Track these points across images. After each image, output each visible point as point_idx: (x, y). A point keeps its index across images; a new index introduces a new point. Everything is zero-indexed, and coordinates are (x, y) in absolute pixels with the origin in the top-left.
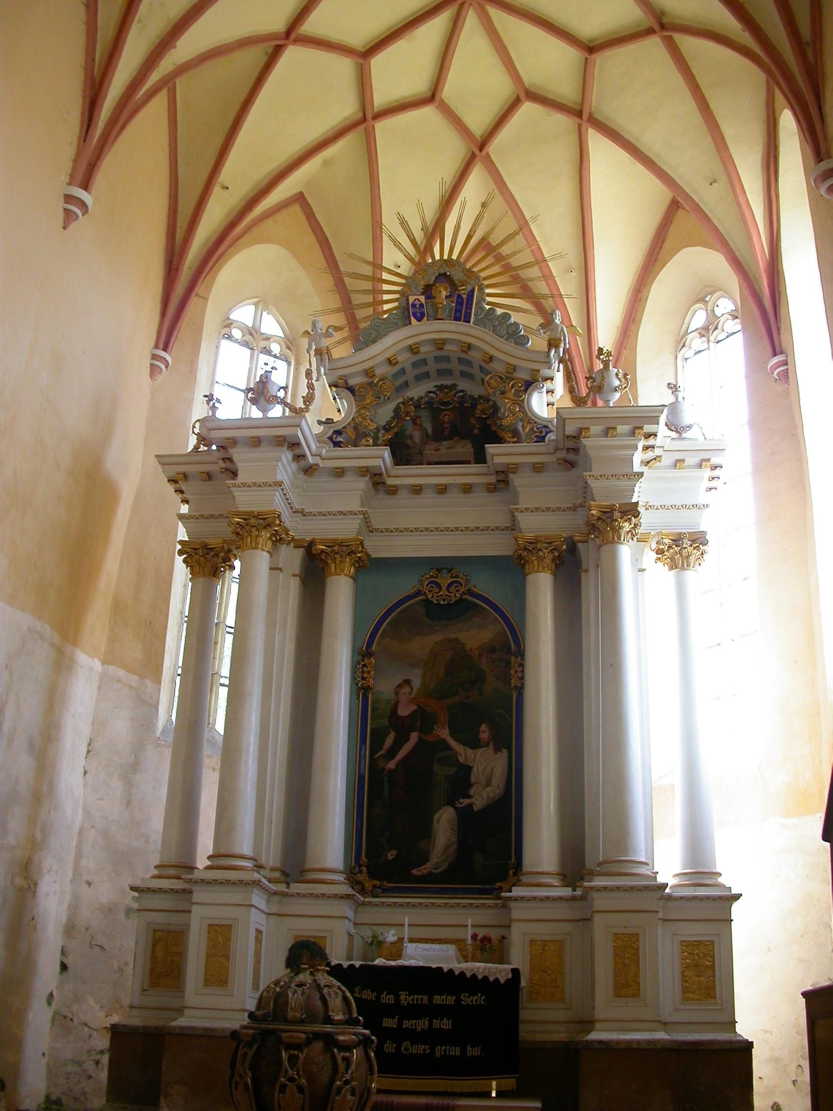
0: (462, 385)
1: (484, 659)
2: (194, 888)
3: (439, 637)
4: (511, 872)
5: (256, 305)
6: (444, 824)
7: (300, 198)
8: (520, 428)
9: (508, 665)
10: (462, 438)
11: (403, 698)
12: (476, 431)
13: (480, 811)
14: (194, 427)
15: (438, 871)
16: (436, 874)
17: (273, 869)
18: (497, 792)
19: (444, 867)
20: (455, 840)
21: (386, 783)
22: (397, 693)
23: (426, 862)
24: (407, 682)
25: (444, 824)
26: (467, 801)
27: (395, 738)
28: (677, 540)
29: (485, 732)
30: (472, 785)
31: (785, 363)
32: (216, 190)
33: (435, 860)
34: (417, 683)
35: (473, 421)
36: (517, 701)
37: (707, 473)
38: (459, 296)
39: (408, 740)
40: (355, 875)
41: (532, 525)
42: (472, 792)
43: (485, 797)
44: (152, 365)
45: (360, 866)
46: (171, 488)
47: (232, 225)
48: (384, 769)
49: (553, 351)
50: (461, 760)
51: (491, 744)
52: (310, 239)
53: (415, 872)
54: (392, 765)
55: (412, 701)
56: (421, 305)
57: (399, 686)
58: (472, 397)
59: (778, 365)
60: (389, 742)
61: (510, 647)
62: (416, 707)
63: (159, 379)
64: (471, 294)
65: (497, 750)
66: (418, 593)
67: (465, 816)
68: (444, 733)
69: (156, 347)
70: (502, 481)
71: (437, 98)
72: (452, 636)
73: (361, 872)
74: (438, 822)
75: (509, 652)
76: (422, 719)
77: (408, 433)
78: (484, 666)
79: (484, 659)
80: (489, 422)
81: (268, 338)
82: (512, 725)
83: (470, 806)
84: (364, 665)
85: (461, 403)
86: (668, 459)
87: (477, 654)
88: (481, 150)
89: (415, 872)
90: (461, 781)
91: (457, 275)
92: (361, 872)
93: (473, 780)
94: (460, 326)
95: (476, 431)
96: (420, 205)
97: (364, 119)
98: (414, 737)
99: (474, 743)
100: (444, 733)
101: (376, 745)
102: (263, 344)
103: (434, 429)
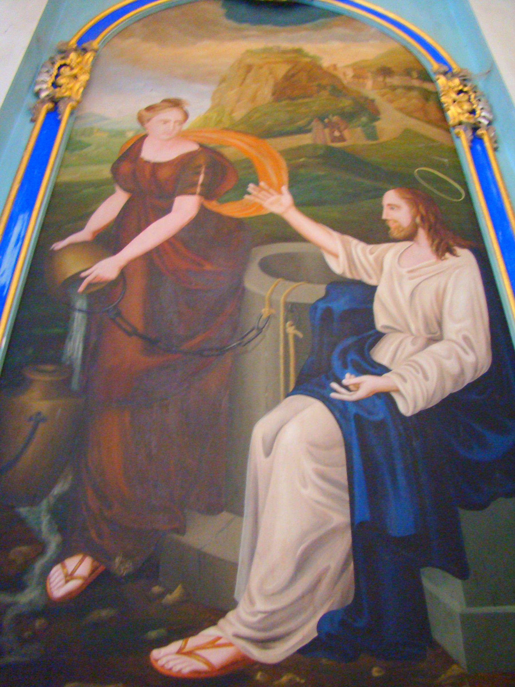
1: (369, 83)
13: (423, 415)
18: (470, 359)
20: (340, 517)
26: (368, 384)
27: (125, 212)
30: (379, 336)
34: (199, 104)
42: (382, 354)
43: (433, 373)
50: (338, 266)
51: (422, 234)
57: (150, 109)
60: (107, 212)
62: (194, 147)
65: (443, 248)
67: (370, 433)
68: (278, 202)
74: (268, 452)
78: (369, 89)
79: (369, 83)
82: (469, 199)
83: (386, 398)
87: (350, 73)
89: (169, 658)
93: (381, 321)
98: (185, 207)
100: (278, 202)
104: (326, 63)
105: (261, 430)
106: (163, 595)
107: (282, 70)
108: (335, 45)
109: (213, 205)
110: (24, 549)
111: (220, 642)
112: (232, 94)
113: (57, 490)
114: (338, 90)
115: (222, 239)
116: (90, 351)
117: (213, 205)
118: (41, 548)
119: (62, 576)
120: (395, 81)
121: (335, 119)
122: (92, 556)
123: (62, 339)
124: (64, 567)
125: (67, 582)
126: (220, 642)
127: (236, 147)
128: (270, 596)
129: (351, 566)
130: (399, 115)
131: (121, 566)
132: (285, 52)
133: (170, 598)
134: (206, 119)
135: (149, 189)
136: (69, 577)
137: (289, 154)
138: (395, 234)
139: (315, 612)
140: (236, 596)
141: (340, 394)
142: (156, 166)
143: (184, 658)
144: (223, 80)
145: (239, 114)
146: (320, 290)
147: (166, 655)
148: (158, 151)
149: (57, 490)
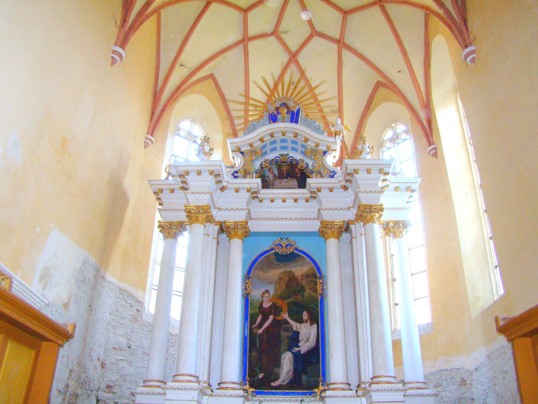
0: (292, 154)
1: (304, 281)
2: (167, 392)
3: (281, 270)
4: (321, 383)
5: (191, 121)
6: (287, 361)
7: (212, 76)
8: (322, 171)
9: (316, 283)
10: (292, 178)
11: (266, 299)
12: (298, 175)
13: (304, 354)
14: (166, 169)
15: (284, 384)
16: (284, 385)
17: (204, 382)
18: (312, 344)
19: (287, 381)
20: (292, 368)
21: (258, 340)
22: (262, 297)
24: (267, 291)
25: (287, 361)
26: (297, 349)
27: (262, 320)
28: (396, 223)
29: (305, 316)
30: (299, 341)
31: (436, 148)
32: (177, 66)
34: (272, 292)
35: (297, 170)
36: (321, 300)
37: (409, 193)
38: (293, 112)
39: (268, 319)
41: (327, 216)
42: (300, 344)
43: (306, 347)
44: (145, 142)
46: (154, 197)
47: (183, 83)
48: (256, 333)
49: (337, 137)
50: (294, 329)
52: (216, 94)
53: (273, 384)
54: (260, 331)
55: (270, 300)
56: (275, 116)
57: (263, 293)
58: (296, 160)
59: (433, 149)
61: (316, 275)
63: (148, 149)
64: (299, 109)
65: (312, 324)
66: (272, 249)
67: (297, 357)
68: (286, 316)
69: (148, 134)
70: (314, 196)
71: (276, 32)
72: (288, 270)
75: (316, 277)
76: (275, 309)
77: (266, 175)
78: (304, 283)
79: (304, 281)
80: (304, 171)
81: (196, 137)
83: (299, 351)
84: (246, 283)
85: (291, 162)
86: (392, 186)
88: (294, 57)
90: (295, 339)
91: (291, 104)
93: (300, 338)
94: (294, 125)
95: (298, 175)
96: (272, 74)
97: (243, 40)
98: (271, 318)
99: (300, 321)
100: (286, 316)
101: (253, 322)
102: (194, 139)
103: (279, 173)
104: (296, 275)
105: (283, 356)
107: (287, 279)
108: (298, 268)
109: (275, 317)
112: (277, 287)
113: (259, 365)
114: (298, 284)
115: (278, 324)
116: (260, 346)
117: (275, 317)
120: (309, 279)
121: (296, 293)
123: (256, 343)
127: (279, 303)
130: (309, 290)
132: (288, 272)
134: (273, 295)
135: (265, 313)
137: (288, 304)
138: (304, 321)
141: (294, 351)
142: (266, 308)
144: (276, 283)
145: (279, 293)
146: (291, 333)
148: (266, 305)
149: (259, 365)
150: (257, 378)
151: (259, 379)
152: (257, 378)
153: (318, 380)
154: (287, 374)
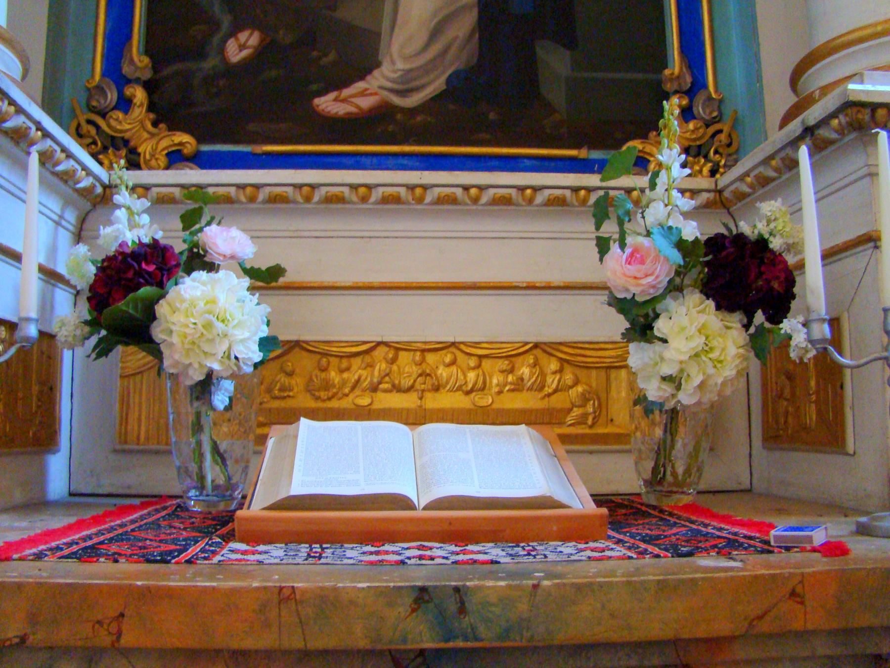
4: (672, 107)
19: (437, 85)
23: (369, 71)
33: (401, 65)
40: (104, 115)
45: (121, 82)
53: (328, 104)
73: (125, 104)
89: (328, 104)
92: (125, 104)
106: (320, 58)
110: (203, 27)
111: (368, 92)
118: (215, 25)
119: (236, 46)
122: (261, 31)
124: (237, 39)
125: (241, 51)
126: (368, 92)
128: (407, 59)
129: (477, 35)
131: (285, 37)
133: (325, 61)
136: (242, 47)
139: (444, 72)
140: (380, 58)
143: (339, 104)
147: (326, 102)
150: (210, 64)
151: (231, 71)
152: (210, 64)
153: (659, 83)
154: (435, 34)
